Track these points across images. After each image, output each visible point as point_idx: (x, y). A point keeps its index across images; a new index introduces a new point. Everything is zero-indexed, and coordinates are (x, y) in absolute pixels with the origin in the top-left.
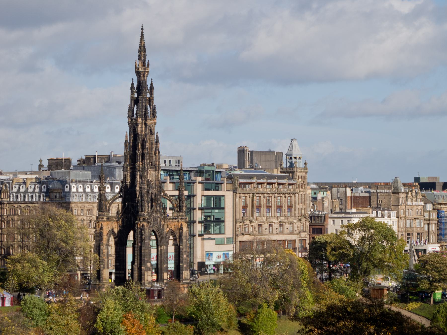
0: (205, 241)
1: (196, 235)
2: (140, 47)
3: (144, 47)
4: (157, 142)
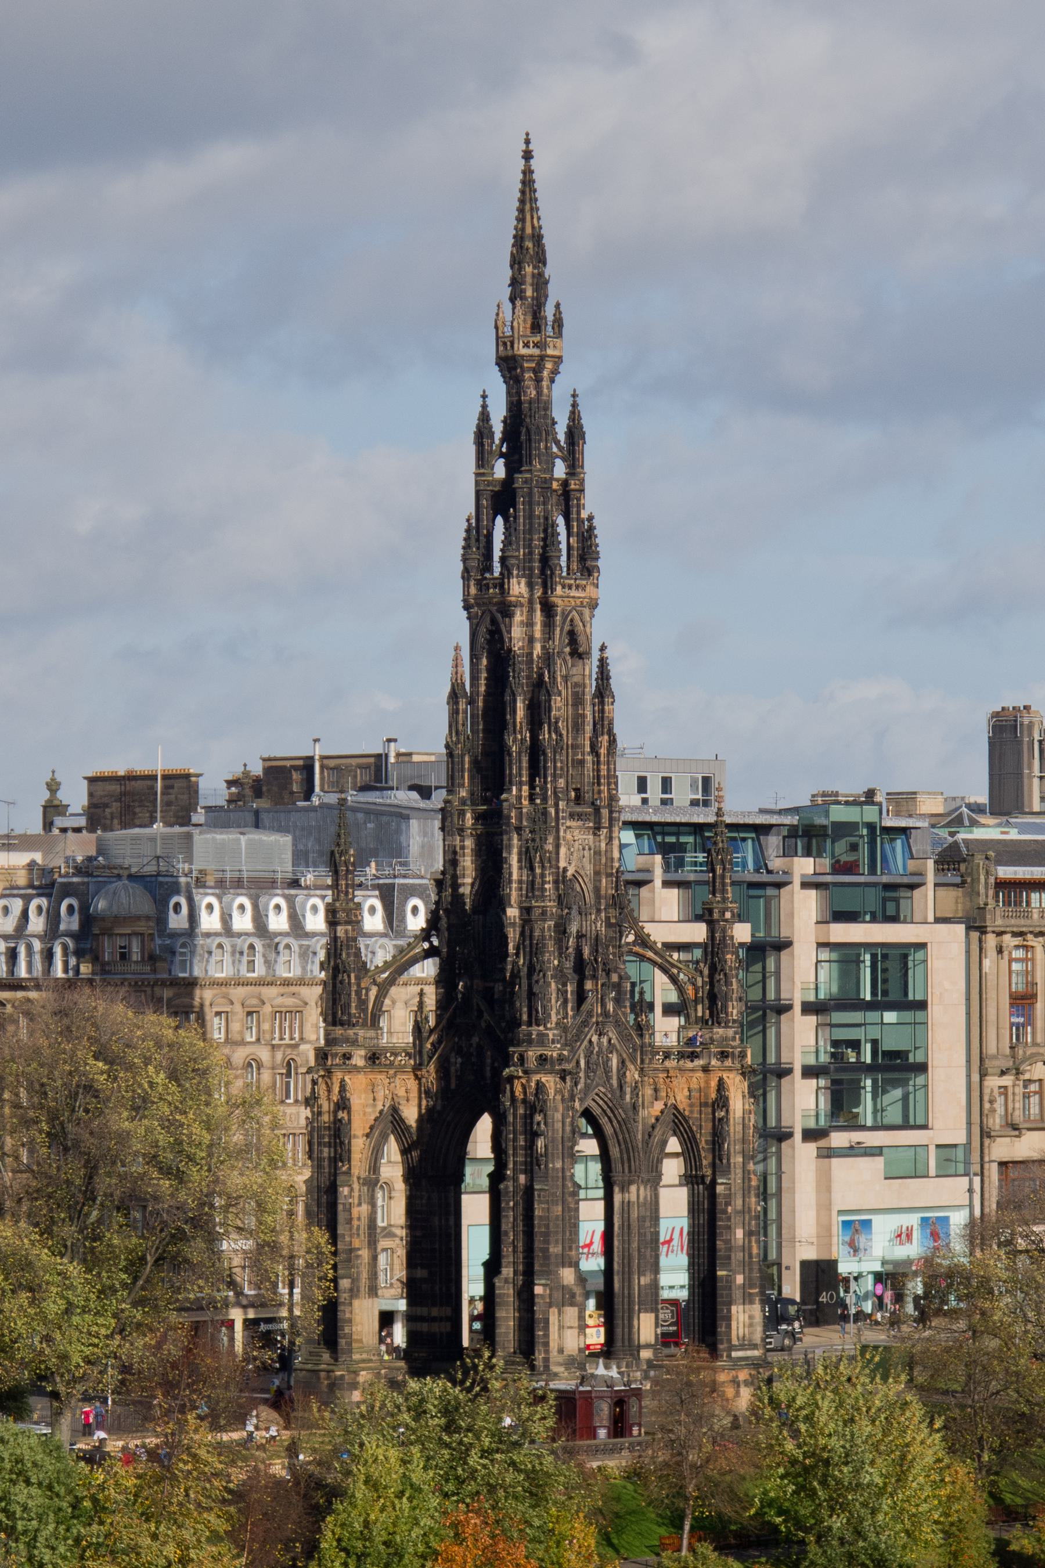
0: (834, 1160)
1: (790, 1135)
2: (519, 239)
3: (538, 238)
4: (603, 691)
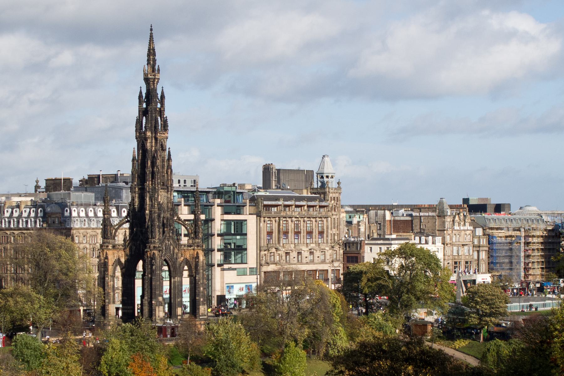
2: (149, 50)
3: (154, 50)
4: (169, 159)
